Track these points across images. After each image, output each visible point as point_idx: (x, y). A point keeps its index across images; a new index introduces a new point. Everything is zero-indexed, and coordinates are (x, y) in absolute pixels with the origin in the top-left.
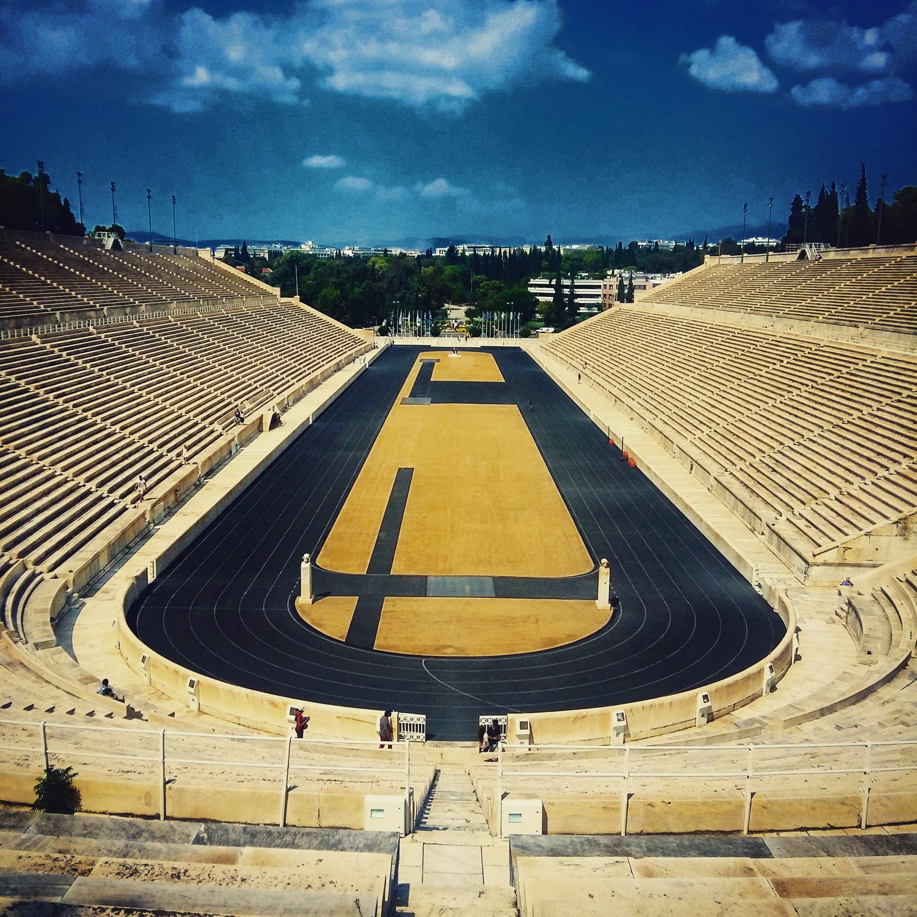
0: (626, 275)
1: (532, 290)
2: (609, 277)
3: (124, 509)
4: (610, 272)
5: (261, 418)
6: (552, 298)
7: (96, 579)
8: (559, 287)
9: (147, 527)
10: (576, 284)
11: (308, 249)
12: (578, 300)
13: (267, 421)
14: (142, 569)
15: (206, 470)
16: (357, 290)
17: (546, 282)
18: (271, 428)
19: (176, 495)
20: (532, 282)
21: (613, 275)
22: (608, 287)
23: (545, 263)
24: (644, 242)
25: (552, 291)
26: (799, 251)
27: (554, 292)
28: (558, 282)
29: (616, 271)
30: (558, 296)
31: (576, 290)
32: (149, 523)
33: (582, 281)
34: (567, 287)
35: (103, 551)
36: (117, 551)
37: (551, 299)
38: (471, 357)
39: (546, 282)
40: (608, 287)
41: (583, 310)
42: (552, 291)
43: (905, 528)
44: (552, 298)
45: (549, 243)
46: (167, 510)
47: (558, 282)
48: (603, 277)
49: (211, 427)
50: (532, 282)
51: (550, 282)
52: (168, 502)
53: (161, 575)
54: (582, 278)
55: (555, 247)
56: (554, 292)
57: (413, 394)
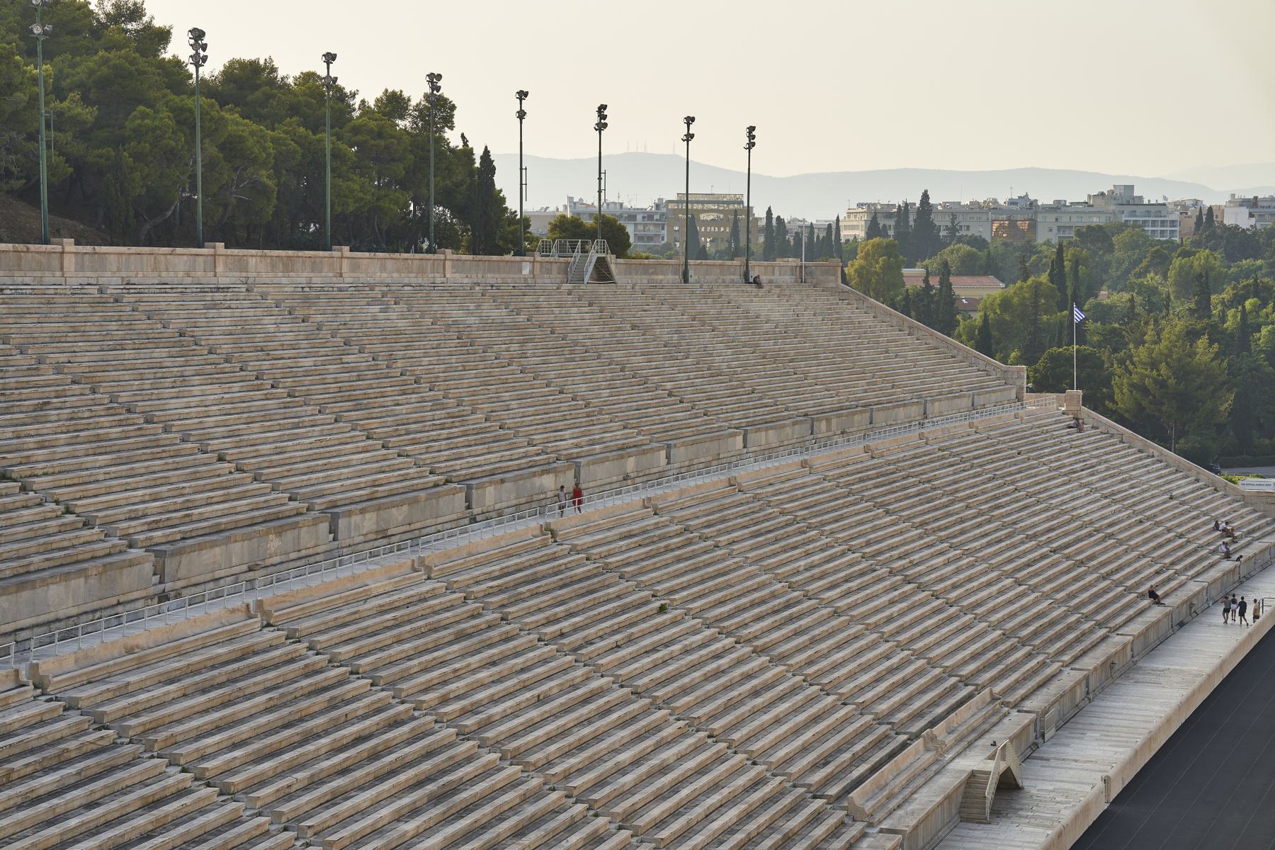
5: (973, 779)
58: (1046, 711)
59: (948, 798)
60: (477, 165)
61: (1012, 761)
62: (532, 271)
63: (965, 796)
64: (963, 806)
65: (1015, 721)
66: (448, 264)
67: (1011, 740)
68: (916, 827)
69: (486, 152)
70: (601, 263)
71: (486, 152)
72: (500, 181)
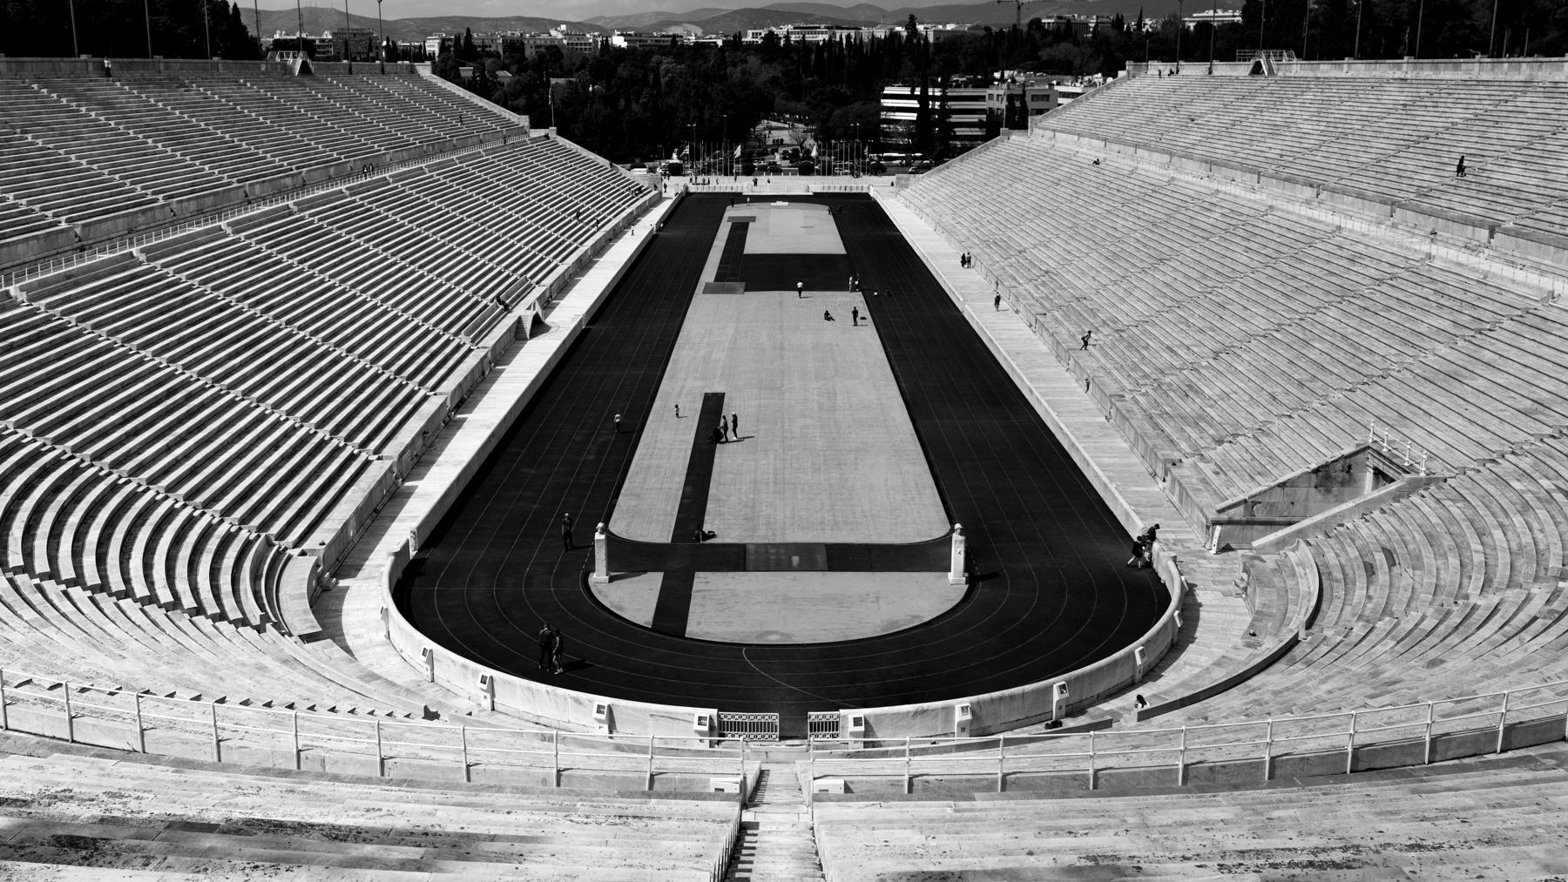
0: (1021, 78)
1: (887, 103)
2: (996, 83)
3: (367, 463)
4: (997, 75)
5: (519, 321)
6: (916, 115)
7: (345, 553)
8: (923, 99)
9: (395, 483)
10: (949, 94)
11: (560, 36)
12: (955, 118)
13: (528, 325)
14: (403, 542)
15: (456, 401)
16: (636, 107)
17: (907, 91)
18: (533, 335)
19: (424, 438)
20: (888, 90)
21: (1002, 80)
22: (995, 97)
23: (908, 63)
24: (1049, 18)
25: (915, 104)
26: (1252, 61)
27: (918, 106)
28: (925, 92)
29: (1007, 73)
30: (923, 111)
31: (949, 103)
32: (396, 478)
33: (957, 90)
34: (934, 98)
35: (350, 519)
36: (365, 517)
37: (913, 116)
38: (800, 214)
39: (907, 91)
40: (995, 97)
41: (960, 131)
42: (915, 104)
43: (1327, 477)
44: (916, 115)
45: (911, 25)
46: (415, 461)
47: (925, 92)
48: (988, 83)
49: (457, 341)
50: (888, 90)
51: (913, 91)
52: (415, 449)
53: (422, 548)
54: (958, 86)
55: (920, 28)
56: (918, 106)
57: (720, 277)
58: (551, 285)
59: (509, 330)
60: (231, 11)
61: (538, 309)
62: (267, 69)
63: (517, 328)
64: (516, 333)
65: (538, 291)
66: (220, 65)
67: (538, 299)
68: (495, 345)
69: (235, 5)
70: (304, 64)
71: (235, 5)
72: (244, 20)
